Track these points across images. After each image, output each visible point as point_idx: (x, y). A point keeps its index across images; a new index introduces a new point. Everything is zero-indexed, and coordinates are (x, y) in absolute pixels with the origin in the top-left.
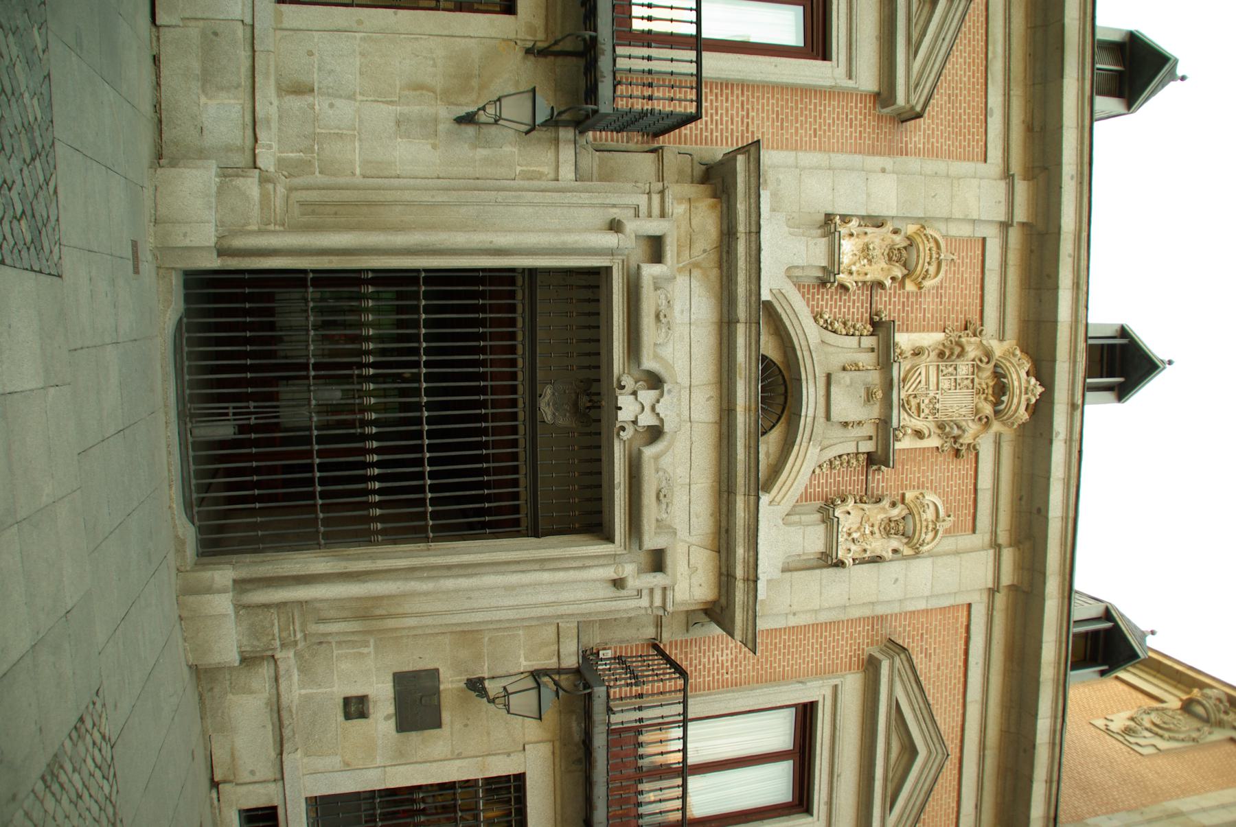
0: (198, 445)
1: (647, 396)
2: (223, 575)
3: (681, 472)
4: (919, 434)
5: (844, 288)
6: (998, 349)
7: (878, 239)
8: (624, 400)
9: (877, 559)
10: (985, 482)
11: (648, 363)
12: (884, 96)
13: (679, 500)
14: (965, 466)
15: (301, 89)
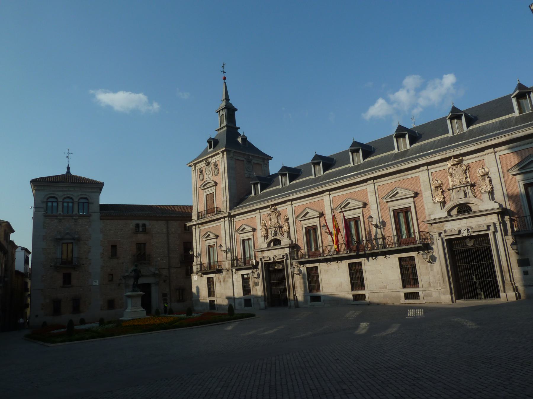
0: (485, 298)
1: (462, 232)
2: (502, 294)
3: (475, 224)
4: (466, 178)
5: (444, 198)
6: (449, 166)
7: (435, 194)
8: (464, 235)
9: (490, 181)
10: (473, 160)
11: (457, 233)
12: (414, 197)
13: (480, 223)
14: (471, 165)
15: (430, 284)
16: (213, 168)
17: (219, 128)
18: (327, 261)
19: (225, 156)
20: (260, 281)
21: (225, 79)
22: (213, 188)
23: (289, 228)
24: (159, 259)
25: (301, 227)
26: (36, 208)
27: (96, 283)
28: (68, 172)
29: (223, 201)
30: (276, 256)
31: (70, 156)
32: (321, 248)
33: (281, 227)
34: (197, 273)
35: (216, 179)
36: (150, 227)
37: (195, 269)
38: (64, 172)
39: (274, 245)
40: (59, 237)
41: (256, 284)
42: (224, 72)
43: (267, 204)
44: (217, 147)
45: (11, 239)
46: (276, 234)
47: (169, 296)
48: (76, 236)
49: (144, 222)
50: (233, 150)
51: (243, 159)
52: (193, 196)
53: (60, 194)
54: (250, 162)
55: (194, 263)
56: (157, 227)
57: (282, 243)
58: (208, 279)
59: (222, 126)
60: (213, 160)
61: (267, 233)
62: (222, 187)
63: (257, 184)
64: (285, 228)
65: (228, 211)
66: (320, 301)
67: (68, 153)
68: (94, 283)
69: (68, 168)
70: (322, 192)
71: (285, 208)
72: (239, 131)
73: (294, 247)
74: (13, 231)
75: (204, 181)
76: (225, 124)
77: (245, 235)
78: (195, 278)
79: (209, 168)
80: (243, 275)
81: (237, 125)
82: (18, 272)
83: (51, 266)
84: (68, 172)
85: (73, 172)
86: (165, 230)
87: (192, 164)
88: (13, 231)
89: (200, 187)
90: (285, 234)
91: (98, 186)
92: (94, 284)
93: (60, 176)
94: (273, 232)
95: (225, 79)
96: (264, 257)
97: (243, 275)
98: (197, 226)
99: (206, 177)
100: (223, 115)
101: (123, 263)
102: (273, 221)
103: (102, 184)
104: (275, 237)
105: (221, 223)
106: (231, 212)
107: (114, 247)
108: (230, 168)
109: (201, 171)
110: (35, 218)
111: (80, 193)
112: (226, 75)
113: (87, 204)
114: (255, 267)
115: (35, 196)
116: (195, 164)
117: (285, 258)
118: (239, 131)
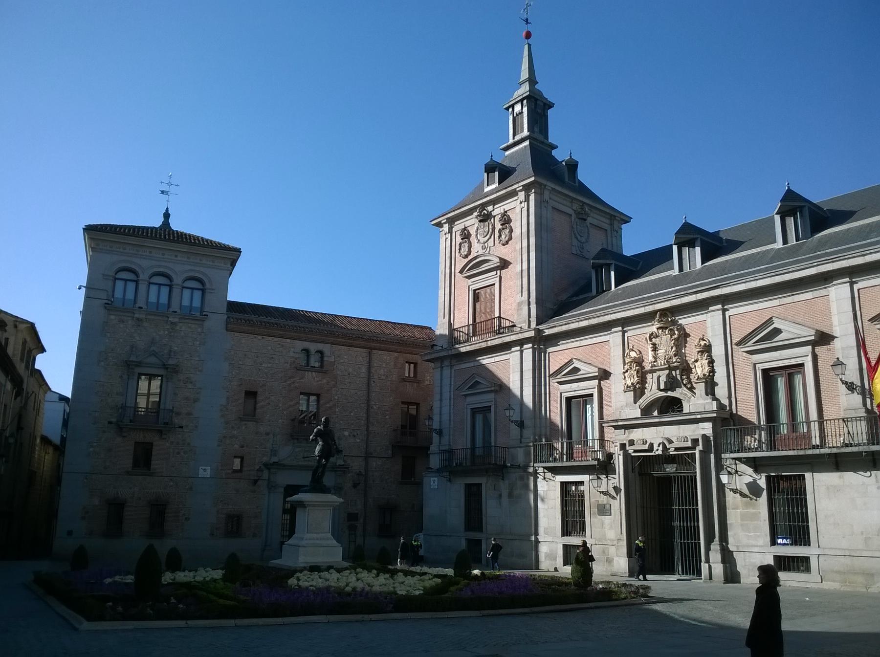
16: (498, 226)
17: (511, 141)
18: (839, 462)
19: (532, 197)
20: (618, 505)
21: (528, 35)
22: (494, 273)
23: (713, 371)
24: (346, 433)
25: (750, 369)
26: (91, 288)
27: (205, 472)
28: (166, 223)
29: (520, 304)
30: (670, 442)
31: (172, 189)
32: (815, 427)
33: (686, 370)
34: (439, 471)
35: (505, 252)
36: (332, 359)
37: (435, 461)
38: (156, 222)
39: (662, 412)
40: (133, 358)
41: (603, 510)
42: (527, 21)
43: (650, 309)
44: (505, 183)
45: (37, 367)
46: (672, 384)
47: (361, 520)
48: (171, 362)
49: (320, 346)
50: (551, 185)
51: (570, 211)
52: (441, 292)
53: (145, 264)
54: (585, 220)
55: (434, 448)
56: (348, 360)
57: (686, 410)
58: (468, 487)
59: (518, 138)
60: (498, 210)
61: (643, 380)
62: (519, 268)
63: (609, 265)
64: (700, 369)
65: (533, 325)
66: (808, 570)
67: (170, 184)
68: (201, 471)
69: (167, 215)
70: (826, 279)
71: (700, 318)
72: (554, 153)
73: (727, 422)
74: (43, 350)
75: (470, 257)
76: (526, 133)
77: (574, 386)
78: (432, 482)
79: (485, 227)
80: (564, 485)
81: (551, 140)
82: (45, 440)
83: (110, 423)
84: (166, 223)
85: (176, 225)
86: (364, 370)
87: (443, 219)
88: (43, 350)
89: (461, 272)
90: (700, 388)
91: (230, 256)
92: (201, 474)
93: (149, 228)
94: (663, 379)
95: (528, 35)
96: (632, 443)
97: (564, 485)
98: (446, 363)
99: (477, 249)
100: (521, 113)
101: (267, 434)
102: (661, 352)
103: (239, 251)
104: (670, 394)
105: (513, 356)
106: (541, 327)
107: (251, 395)
108: (542, 228)
109: (466, 235)
110: (85, 313)
111: (189, 267)
112: (530, 28)
113: (200, 293)
114: (605, 467)
115: (92, 265)
116: (451, 221)
117: (700, 447)
118: (554, 153)
